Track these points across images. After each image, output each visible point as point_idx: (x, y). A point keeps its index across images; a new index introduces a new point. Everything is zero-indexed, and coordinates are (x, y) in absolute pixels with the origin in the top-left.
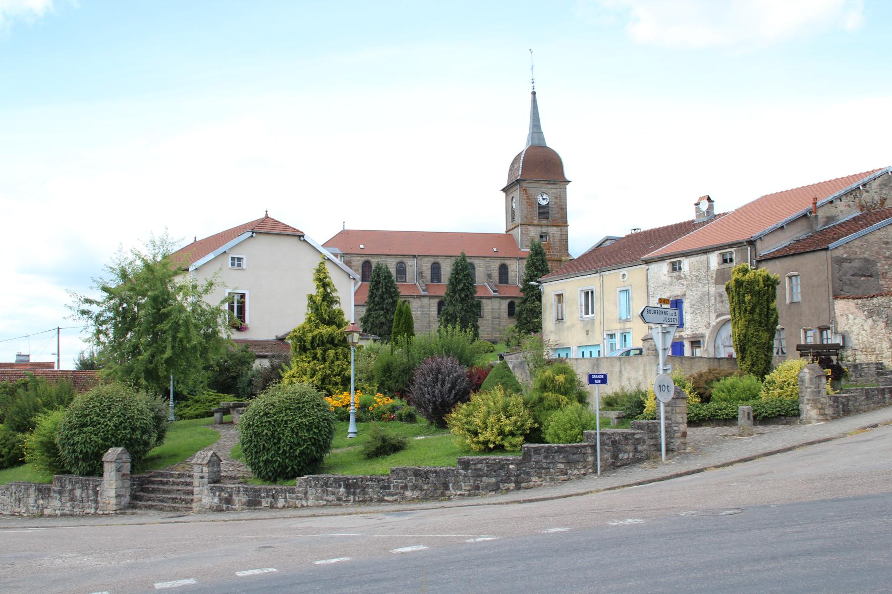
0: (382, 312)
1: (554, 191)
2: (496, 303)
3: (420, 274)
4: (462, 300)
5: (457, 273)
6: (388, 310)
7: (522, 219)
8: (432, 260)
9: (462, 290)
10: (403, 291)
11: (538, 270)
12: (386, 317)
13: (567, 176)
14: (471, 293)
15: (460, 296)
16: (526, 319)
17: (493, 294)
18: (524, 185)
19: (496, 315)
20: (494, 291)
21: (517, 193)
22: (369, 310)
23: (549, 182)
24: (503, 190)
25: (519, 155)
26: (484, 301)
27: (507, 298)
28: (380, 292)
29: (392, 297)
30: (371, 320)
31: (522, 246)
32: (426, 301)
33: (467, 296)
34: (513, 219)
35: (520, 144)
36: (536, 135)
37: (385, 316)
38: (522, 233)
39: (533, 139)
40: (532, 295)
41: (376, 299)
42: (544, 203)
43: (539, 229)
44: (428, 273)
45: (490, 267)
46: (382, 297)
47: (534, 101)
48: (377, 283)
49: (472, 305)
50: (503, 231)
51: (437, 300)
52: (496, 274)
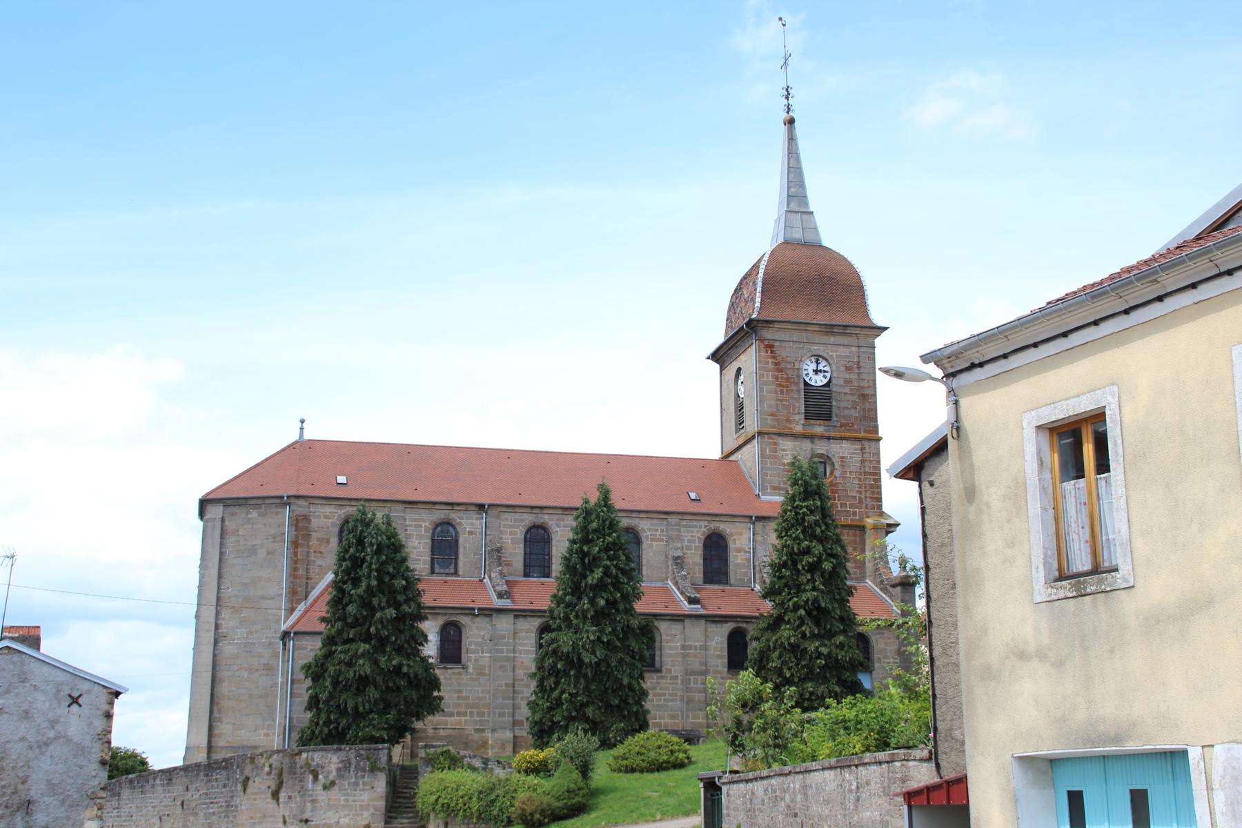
0: (363, 647)
1: (843, 351)
2: (696, 631)
3: (496, 554)
4: (600, 617)
5: (586, 541)
7: (762, 420)
8: (529, 519)
9: (600, 587)
10: (437, 592)
11: (813, 537)
12: (376, 662)
13: (877, 318)
14: (626, 598)
15: (592, 602)
17: (686, 607)
18: (768, 334)
19: (696, 665)
20: (692, 601)
21: (748, 359)
22: (330, 641)
23: (830, 329)
24: (720, 356)
25: (756, 267)
26: (663, 626)
28: (360, 591)
29: (397, 605)
30: (332, 669)
31: (763, 489)
32: (504, 624)
33: (611, 604)
34: (740, 423)
35: (755, 239)
37: (371, 658)
38: (762, 455)
40: (796, 607)
41: (351, 609)
42: (819, 381)
43: (807, 445)
44: (516, 553)
45: (679, 538)
46: (366, 604)
47: (791, 139)
48: (357, 563)
49: (628, 629)
50: (712, 450)
51: (536, 623)
52: (695, 558)
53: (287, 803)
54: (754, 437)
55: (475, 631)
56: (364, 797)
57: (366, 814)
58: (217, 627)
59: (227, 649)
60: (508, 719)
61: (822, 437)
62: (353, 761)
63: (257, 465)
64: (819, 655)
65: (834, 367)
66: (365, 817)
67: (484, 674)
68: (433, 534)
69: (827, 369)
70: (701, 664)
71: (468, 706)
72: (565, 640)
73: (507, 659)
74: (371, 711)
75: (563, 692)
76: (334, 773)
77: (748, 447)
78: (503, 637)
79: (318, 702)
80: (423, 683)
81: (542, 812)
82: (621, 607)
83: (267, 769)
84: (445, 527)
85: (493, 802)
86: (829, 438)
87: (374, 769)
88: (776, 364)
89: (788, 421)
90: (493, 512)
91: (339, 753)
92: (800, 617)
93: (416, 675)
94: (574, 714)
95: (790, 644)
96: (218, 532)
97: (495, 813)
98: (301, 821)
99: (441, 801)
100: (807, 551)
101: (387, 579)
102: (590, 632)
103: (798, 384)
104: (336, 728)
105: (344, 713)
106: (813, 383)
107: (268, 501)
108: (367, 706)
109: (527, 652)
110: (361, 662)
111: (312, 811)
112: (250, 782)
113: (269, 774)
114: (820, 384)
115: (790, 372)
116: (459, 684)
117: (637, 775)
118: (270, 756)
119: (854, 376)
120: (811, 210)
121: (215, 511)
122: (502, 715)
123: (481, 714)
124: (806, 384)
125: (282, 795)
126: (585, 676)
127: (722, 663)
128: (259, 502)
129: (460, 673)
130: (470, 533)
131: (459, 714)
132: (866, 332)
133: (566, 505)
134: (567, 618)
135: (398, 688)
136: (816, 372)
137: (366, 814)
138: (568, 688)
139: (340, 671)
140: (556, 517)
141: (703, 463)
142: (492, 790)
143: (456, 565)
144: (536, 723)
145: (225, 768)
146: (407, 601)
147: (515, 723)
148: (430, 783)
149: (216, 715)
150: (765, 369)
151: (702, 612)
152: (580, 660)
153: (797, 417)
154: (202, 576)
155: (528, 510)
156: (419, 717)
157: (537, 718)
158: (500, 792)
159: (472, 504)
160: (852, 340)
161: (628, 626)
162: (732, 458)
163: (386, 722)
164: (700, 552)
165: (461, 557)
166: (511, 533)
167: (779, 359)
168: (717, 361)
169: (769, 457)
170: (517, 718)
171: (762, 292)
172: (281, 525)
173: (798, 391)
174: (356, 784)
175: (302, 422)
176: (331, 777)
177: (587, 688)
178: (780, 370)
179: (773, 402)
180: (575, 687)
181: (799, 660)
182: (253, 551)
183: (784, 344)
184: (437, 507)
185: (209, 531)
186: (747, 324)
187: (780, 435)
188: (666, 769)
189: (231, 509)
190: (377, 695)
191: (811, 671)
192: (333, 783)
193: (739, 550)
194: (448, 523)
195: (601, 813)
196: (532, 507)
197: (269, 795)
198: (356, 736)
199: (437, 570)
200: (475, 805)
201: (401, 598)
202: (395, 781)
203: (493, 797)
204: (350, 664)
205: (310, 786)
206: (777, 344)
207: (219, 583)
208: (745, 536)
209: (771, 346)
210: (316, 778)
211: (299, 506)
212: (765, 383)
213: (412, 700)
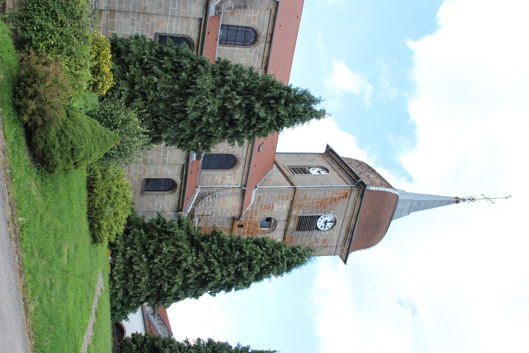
8: (263, 32)
9: (249, 111)
13: (353, 256)
16: (158, 251)
18: (354, 194)
21: (337, 181)
24: (330, 152)
25: (390, 187)
33: (233, 123)
36: (408, 205)
38: (281, 191)
42: (320, 223)
43: (284, 217)
51: (194, 36)
54: (292, 184)
60: (117, 6)
61: (287, 227)
64: (172, 285)
65: (327, 233)
69: (326, 228)
70: (152, 160)
72: (206, 82)
73: (167, 9)
75: (157, 77)
77: (284, 178)
78: (185, 8)
81: (41, 112)
82: (230, 132)
85: (54, 16)
86: (286, 230)
88: (335, 199)
89: (300, 206)
92: (200, 268)
95: (180, 262)
97: (38, 20)
100: (250, 268)
102: (213, 107)
103: (321, 212)
106: (319, 220)
109: (171, 27)
114: (318, 224)
115: (329, 207)
117: (84, 193)
119: (320, 244)
120: (410, 214)
124: (319, 216)
126: (173, 101)
127: (151, 174)
132: (345, 251)
133: (271, 61)
134: (224, 82)
136: (326, 222)
138: (163, 82)
140: (262, 52)
141: (274, 148)
142: (72, 15)
144: (127, 46)
147: (112, 12)
151: (191, 161)
152: (190, 94)
153: (301, 211)
155: (270, 32)
157: (133, 48)
158: (68, 30)
160: (341, 243)
161: (212, 136)
162: (274, 165)
166: (254, 17)
169: (279, 196)
170: (117, 14)
171: (378, 191)
173: (317, 212)
177: (161, 99)
179: (313, 197)
180: (163, 89)
181: (167, 268)
183: (346, 204)
186: (362, 182)
187: (292, 202)
188: (91, 227)
191: (157, 278)
193: (223, 178)
195: (39, 199)
196: (272, 35)
203: (61, 17)
206: (347, 200)
208: (233, 182)
209: (346, 197)
212: (325, 193)
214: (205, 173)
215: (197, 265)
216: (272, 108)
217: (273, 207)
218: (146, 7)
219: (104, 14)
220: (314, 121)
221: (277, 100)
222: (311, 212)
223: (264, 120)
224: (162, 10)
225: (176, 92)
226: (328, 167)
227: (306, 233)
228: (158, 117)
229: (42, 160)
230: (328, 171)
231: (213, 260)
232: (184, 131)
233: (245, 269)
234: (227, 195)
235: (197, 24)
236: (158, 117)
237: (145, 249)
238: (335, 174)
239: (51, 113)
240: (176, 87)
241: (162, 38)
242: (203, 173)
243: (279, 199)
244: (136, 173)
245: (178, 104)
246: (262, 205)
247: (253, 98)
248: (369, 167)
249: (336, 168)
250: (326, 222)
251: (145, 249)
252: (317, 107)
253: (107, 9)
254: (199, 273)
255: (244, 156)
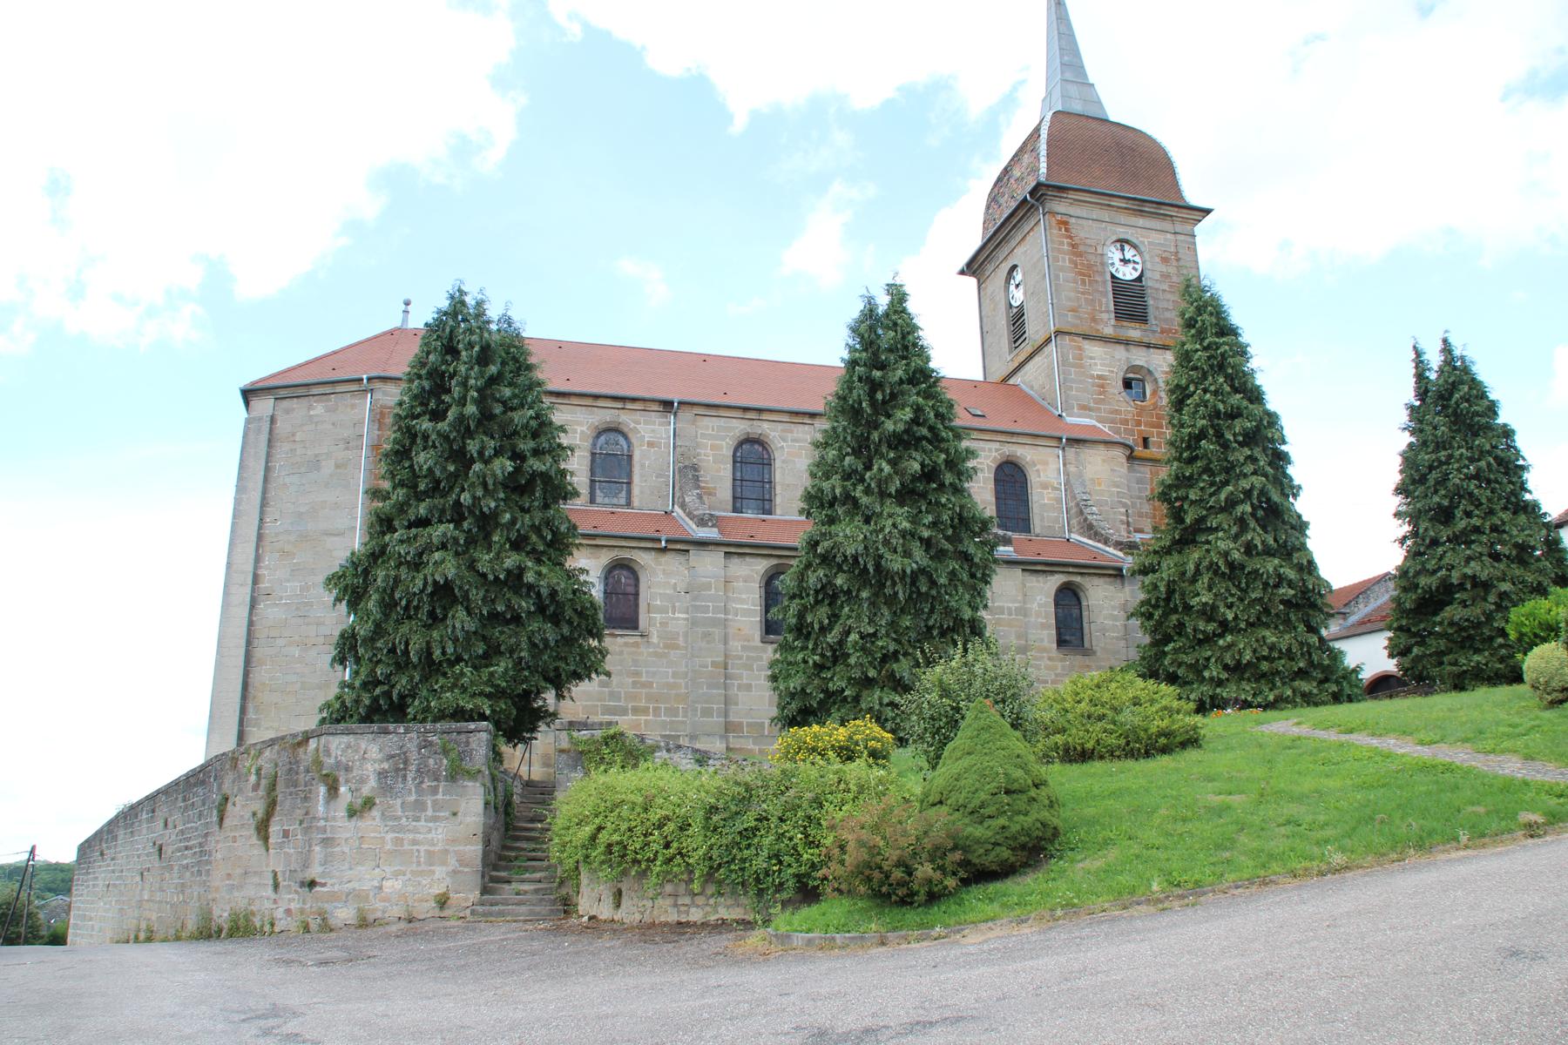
1: (1157, 238)
3: (689, 472)
6: (487, 522)
9: (903, 442)
13: (1193, 195)
16: (1209, 613)
21: (1034, 246)
24: (974, 267)
25: (1037, 130)
27: (1049, 568)
32: (709, 564)
33: (929, 474)
36: (1073, 90)
37: (463, 550)
38: (1063, 362)
39: (1065, 96)
40: (1231, 503)
41: (423, 459)
42: (1128, 273)
43: (1120, 352)
44: (719, 475)
51: (760, 566)
53: (281, 846)
54: (1048, 341)
55: (660, 578)
56: (439, 834)
57: (440, 871)
58: (256, 579)
59: (270, 612)
62: (413, 756)
63: (335, 353)
64: (1281, 579)
65: (1147, 257)
66: (438, 880)
67: (677, 647)
68: (594, 445)
69: (1137, 259)
71: (649, 698)
72: (849, 535)
73: (714, 622)
74: (459, 659)
75: (848, 633)
76: (373, 782)
77: (1037, 359)
79: (353, 648)
80: (569, 613)
81: (937, 853)
82: (948, 478)
83: (253, 778)
84: (612, 436)
86: (1148, 346)
87: (456, 773)
89: (1094, 320)
90: (686, 415)
91: (383, 739)
92: (1242, 522)
93: (553, 593)
94: (872, 673)
96: (264, 437)
97: (760, 863)
98: (302, 884)
99: (603, 837)
100: (1234, 414)
101: (498, 409)
102: (898, 517)
103: (1102, 274)
104: (388, 694)
105: (402, 665)
106: (1120, 276)
107: (339, 388)
108: (450, 650)
109: (747, 612)
110: (437, 556)
111: (324, 863)
112: (229, 806)
113: (256, 787)
114: (1129, 277)
116: (635, 662)
117: (1096, 766)
118: (261, 752)
119: (1172, 270)
121: (264, 406)
122: (707, 712)
123: (672, 712)
124: (1113, 276)
125: (274, 829)
126: (891, 601)
127: (1048, 636)
128: (328, 389)
129: (636, 645)
130: (651, 444)
131: (636, 711)
132: (1184, 214)
133: (795, 408)
134: (849, 499)
135: (516, 619)
136: (1125, 261)
137: (440, 871)
138: (857, 622)
139: (397, 580)
140: (780, 426)
141: (975, 384)
143: (629, 493)
144: (793, 695)
145: (203, 783)
146: (537, 453)
147: (729, 728)
148: (578, 797)
149: (251, 715)
150: (1059, 251)
151: (1014, 556)
153: (1105, 316)
154: (238, 502)
156: (559, 683)
157: (795, 683)
158: (773, 808)
159: (653, 401)
160: (1167, 225)
161: (960, 516)
162: (1011, 382)
163: (489, 682)
164: (991, 485)
165: (636, 479)
166: (713, 447)
167: (1077, 240)
168: (973, 274)
170: (731, 719)
172: (358, 423)
173: (1105, 282)
174: (419, 806)
175: (407, 303)
176: (366, 791)
177: (892, 624)
178: (1080, 255)
180: (871, 621)
182: (315, 464)
183: (1080, 221)
184: (601, 403)
185: (252, 436)
186: (1032, 193)
187: (1086, 337)
188: (1165, 750)
189: (286, 403)
190: (471, 626)
191: (1266, 611)
192: (369, 803)
193: (1045, 486)
194: (614, 430)
195: (1113, 854)
196: (746, 409)
197: (252, 831)
198: (427, 709)
199: (599, 500)
200: (697, 843)
201: (526, 446)
202: (508, 804)
203: (749, 820)
204: (417, 565)
205: (321, 809)
206: (1073, 220)
207: (262, 513)
208: (1053, 466)
209: (1066, 223)
210: (333, 790)
211: (385, 394)
212: (1062, 269)
213: (545, 641)
214: (1037, 524)
215: (1235, 529)
216: (893, 396)
217: (1100, 377)
218: (714, 664)
219: (735, 742)
220: (911, 306)
221: (874, 386)
222: (1105, 294)
223: (918, 410)
224: (717, 632)
225: (876, 595)
226: (1006, 267)
227: (1150, 302)
228: (930, 629)
229: (1033, 850)
230: (1014, 267)
231: (1223, 496)
232: (953, 573)
233: (1239, 425)
234: (1080, 475)
235: (736, 560)
236: (930, 629)
237: (1208, 640)
238: (1019, 251)
239: (938, 835)
240: (864, 594)
241: (770, 628)
242: (1038, 530)
243: (1081, 366)
244: (1047, 668)
245: (899, 588)
246: (1097, 402)
247: (875, 436)
248: (999, 180)
249: (1006, 250)
250: (1125, 261)
251: (1208, 640)
252: (883, 302)
253: (724, 737)
254: (1252, 524)
255: (997, 445)
